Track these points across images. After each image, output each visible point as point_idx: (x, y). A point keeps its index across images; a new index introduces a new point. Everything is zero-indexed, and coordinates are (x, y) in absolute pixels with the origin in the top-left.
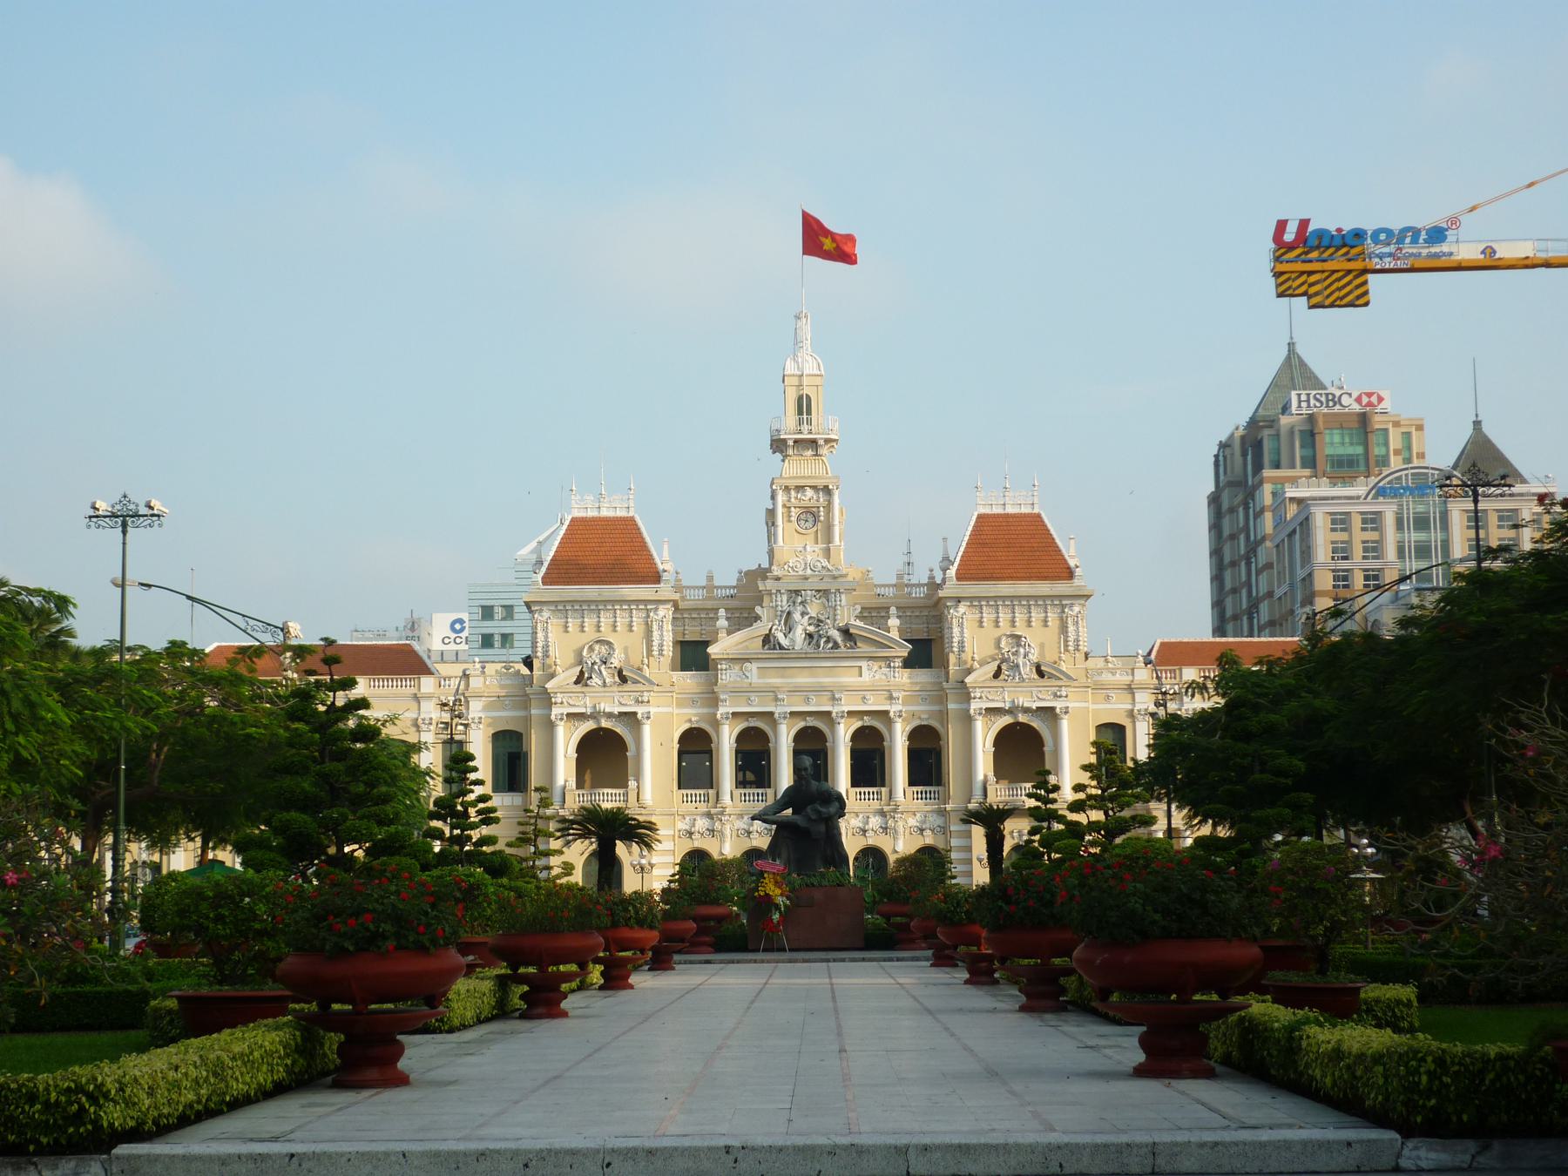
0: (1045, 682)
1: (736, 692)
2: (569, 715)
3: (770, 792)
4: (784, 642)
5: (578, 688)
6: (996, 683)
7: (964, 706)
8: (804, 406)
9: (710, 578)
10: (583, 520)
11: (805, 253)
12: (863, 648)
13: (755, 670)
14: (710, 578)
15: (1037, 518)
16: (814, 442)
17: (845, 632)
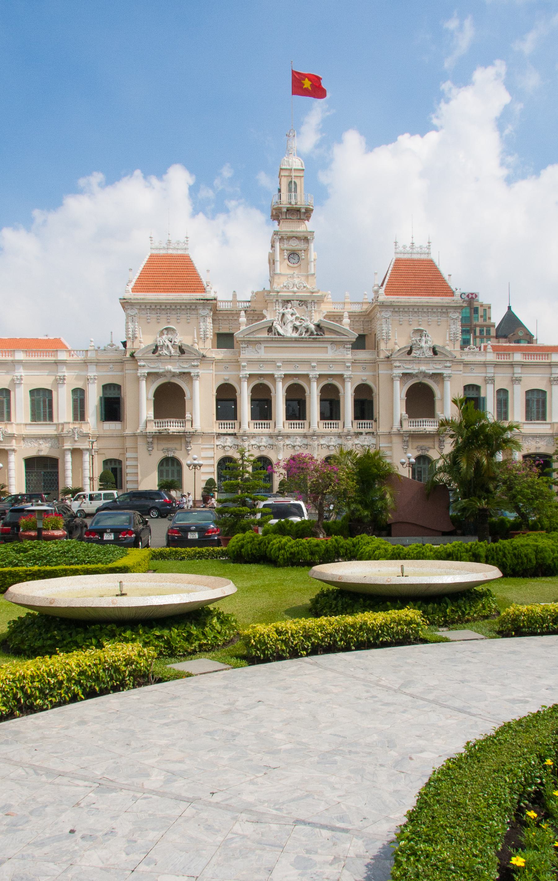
0: (436, 356)
1: (251, 362)
2: (149, 374)
3: (272, 423)
4: (281, 331)
5: (154, 356)
6: (409, 358)
7: (389, 372)
8: (292, 187)
9: (235, 295)
10: (157, 256)
11: (294, 93)
12: (327, 336)
13: (263, 348)
14: (235, 295)
15: (431, 261)
16: (298, 211)
17: (318, 326)
